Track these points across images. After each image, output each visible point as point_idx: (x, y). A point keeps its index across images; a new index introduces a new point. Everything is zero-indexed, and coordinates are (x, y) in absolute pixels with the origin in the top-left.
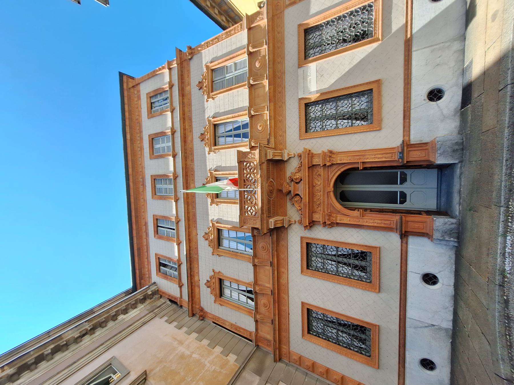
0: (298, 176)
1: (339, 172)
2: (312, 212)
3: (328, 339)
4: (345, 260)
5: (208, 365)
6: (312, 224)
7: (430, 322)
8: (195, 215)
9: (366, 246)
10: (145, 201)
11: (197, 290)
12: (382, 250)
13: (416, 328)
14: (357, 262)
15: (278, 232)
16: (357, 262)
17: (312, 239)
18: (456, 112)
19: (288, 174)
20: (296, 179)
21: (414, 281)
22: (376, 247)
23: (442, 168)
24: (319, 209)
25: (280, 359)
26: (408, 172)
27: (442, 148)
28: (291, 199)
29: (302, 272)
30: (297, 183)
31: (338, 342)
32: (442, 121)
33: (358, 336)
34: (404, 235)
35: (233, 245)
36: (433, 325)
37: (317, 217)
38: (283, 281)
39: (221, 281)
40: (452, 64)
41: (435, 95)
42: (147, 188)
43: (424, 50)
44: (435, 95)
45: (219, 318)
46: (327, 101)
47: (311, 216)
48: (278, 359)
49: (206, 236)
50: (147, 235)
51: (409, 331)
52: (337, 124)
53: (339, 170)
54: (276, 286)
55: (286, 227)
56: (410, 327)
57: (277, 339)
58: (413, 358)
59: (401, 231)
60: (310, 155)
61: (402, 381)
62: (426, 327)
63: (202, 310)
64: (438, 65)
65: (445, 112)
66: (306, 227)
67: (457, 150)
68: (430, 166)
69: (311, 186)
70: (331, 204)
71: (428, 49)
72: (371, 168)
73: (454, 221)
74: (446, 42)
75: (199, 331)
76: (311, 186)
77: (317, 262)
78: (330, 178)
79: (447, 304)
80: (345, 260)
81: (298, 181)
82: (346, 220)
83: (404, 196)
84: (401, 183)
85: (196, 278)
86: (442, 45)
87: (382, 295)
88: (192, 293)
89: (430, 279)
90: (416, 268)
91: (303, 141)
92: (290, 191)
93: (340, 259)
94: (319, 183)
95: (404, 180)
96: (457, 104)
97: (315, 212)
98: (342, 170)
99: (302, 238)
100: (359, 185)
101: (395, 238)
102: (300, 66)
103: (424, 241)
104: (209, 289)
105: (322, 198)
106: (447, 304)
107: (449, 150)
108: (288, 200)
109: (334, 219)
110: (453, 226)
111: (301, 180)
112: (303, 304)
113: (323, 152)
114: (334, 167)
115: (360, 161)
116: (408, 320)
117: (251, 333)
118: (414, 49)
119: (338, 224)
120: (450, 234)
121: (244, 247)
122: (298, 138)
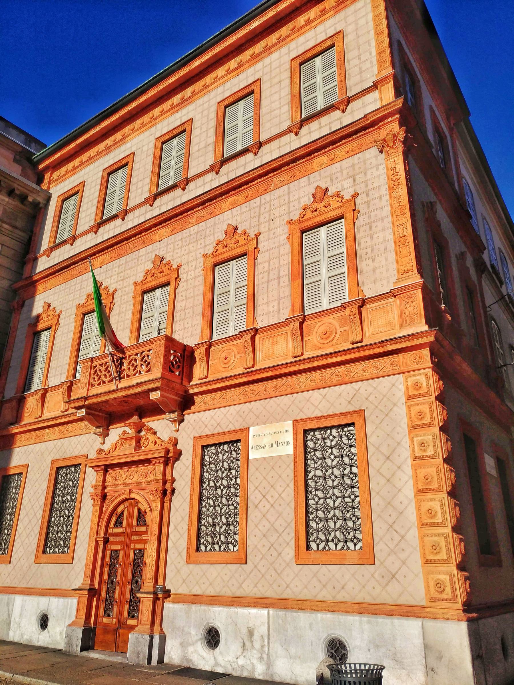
7: (12, 619)
27: (143, 640)
40: (241, 662)
43: (266, 625)
44: (212, 638)
56: (8, 599)
65: (191, 649)
67: (139, 657)
71: (266, 632)
74: (268, 655)
78: (142, 492)
79: (25, 637)
86: (266, 649)
96: (195, 663)
106: (25, 637)
107: (140, 649)
118: (272, 611)
120: (69, 644)
122: (197, 435)
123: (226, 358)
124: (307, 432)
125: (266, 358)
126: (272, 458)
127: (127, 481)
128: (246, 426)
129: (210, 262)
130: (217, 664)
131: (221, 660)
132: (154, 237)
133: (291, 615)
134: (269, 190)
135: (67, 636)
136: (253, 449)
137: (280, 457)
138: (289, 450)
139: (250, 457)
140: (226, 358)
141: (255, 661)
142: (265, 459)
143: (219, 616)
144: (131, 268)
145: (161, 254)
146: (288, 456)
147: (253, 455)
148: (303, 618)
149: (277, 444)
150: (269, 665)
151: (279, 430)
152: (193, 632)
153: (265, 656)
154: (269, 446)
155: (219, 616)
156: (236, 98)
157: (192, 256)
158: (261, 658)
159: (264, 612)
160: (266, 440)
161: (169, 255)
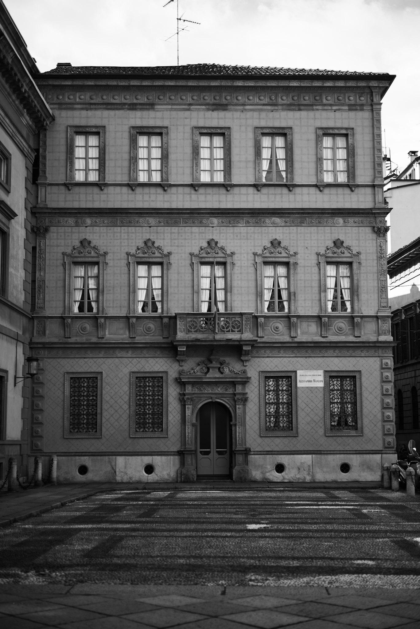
0: (226, 370)
1: (229, 407)
2: (193, 384)
6: (180, 383)
7: (117, 470)
8: (176, 224)
9: (167, 428)
12: (167, 439)
13: (110, 462)
15: (171, 349)
18: (266, 479)
19: (227, 360)
20: (223, 368)
21: (147, 460)
22: (167, 434)
23: (229, 476)
24: (196, 390)
25: (31, 348)
26: (227, 456)
28: (203, 362)
30: (219, 368)
32: (262, 473)
34: (181, 453)
35: (142, 283)
36: (115, 472)
37: (189, 389)
38: (119, 353)
40: (298, 476)
41: (280, 468)
42: (209, 114)
46: (290, 395)
47: (189, 383)
48: (32, 346)
50: (133, 107)
51: (106, 458)
52: (269, 403)
53: (231, 406)
54: (113, 346)
55: (177, 358)
57: (55, 346)
58: (86, 461)
59: (184, 451)
60: (245, 382)
61: (62, 454)
62: (113, 468)
63: (46, 230)
64: (299, 469)
65: (268, 474)
68: (231, 468)
69: (216, 383)
70: (201, 400)
72: (231, 430)
73: (195, 479)
74: (312, 472)
76: (216, 383)
81: (221, 370)
82: (188, 412)
83: (208, 453)
84: (217, 451)
88: (66, 213)
89: (149, 469)
90: (157, 461)
91: (257, 374)
92: (211, 362)
95: (219, 453)
97: (193, 387)
98: (230, 409)
99: (166, 372)
100: (217, 423)
102: (325, 372)
103: (177, 466)
104: (77, 244)
105: (206, 392)
108: (202, 359)
109: (189, 403)
110: (191, 479)
111: (222, 373)
113: (247, 393)
114: (233, 403)
115: (237, 422)
116: (114, 457)
118: (314, 456)
121: (143, 299)
122: (261, 370)
123: (277, 328)
125: (303, 333)
126: (312, 387)
127: (210, 391)
128: (295, 370)
129: (259, 260)
130: (284, 478)
131: (286, 477)
133: (323, 457)
134: (303, 225)
136: (300, 382)
137: (316, 387)
138: (322, 385)
139: (298, 386)
140: (277, 328)
141: (305, 476)
142: (307, 387)
143: (284, 459)
144: (185, 239)
145: (216, 238)
146: (321, 387)
147: (299, 385)
148: (330, 457)
149: (314, 381)
150: (313, 476)
151: (316, 374)
152: (269, 467)
153: (311, 473)
154: (310, 381)
155: (284, 459)
156: (271, 132)
157: (244, 250)
158: (309, 474)
159: (310, 456)
161: (222, 241)
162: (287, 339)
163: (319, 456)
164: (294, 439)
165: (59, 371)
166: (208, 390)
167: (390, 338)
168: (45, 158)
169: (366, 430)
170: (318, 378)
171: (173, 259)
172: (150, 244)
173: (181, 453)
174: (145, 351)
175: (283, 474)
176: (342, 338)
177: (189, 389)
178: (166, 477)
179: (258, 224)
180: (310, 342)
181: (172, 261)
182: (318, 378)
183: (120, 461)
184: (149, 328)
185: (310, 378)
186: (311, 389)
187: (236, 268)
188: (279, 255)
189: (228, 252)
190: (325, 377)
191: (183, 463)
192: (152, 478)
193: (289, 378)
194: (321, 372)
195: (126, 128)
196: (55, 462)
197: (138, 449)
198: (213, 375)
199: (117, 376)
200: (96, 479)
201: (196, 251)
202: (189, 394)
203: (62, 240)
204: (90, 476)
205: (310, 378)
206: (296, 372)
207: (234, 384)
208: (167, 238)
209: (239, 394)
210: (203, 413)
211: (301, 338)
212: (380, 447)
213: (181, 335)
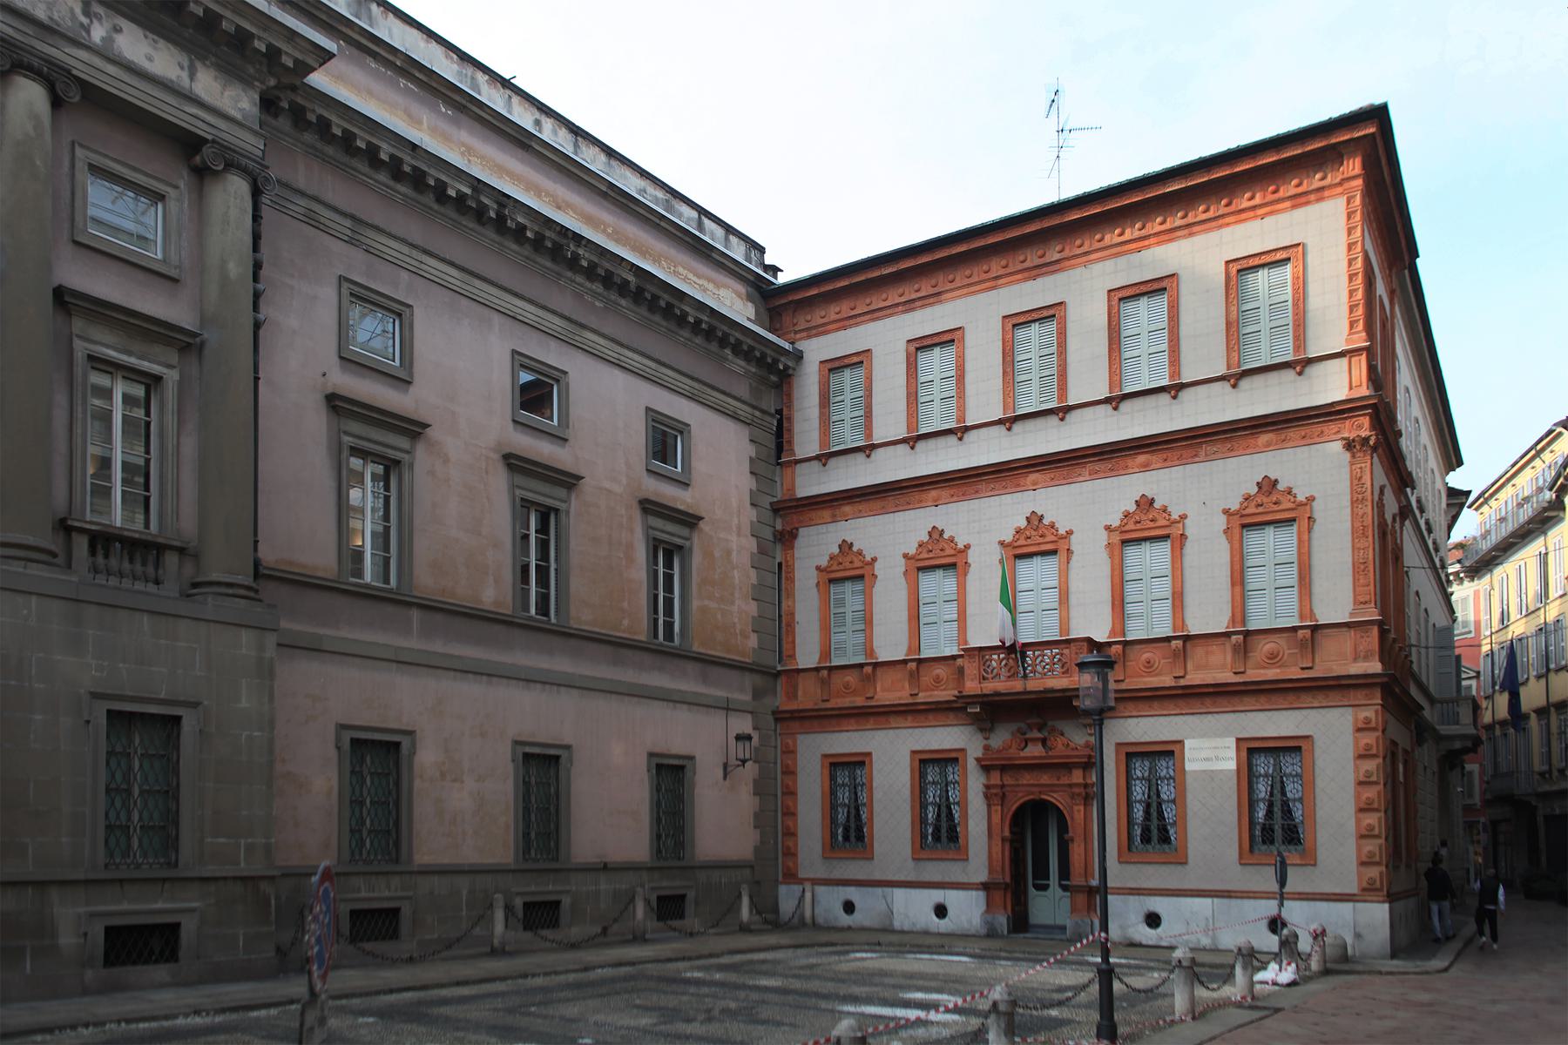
2: (1004, 769)
3: (833, 793)
4: (943, 815)
5: (735, 608)
6: (986, 768)
8: (976, 495)
10: (994, 283)
11: (826, 514)
14: (944, 831)
16: (944, 831)
17: (965, 768)
21: (937, 896)
29: (914, 752)
30: (1044, 741)
31: (833, 807)
33: (850, 832)
34: (985, 887)
38: (894, 721)
39: (861, 577)
41: (1153, 920)
45: (793, 581)
49: (936, 536)
51: (879, 891)
58: (852, 893)
66: (978, 760)
75: (762, 551)
77: (932, 774)
80: (943, 815)
83: (1045, 888)
85: (847, 509)
87: (910, 863)
89: (941, 911)
90: (952, 898)
93: (944, 809)
94: (1045, 779)
99: (963, 750)
101: (983, 876)
102: (1238, 740)
103: (984, 908)
112: (869, 754)
117: (793, 656)
119: (989, 806)
124: (1252, 750)
129: (1117, 538)
132: (1022, 481)
133: (1234, 902)
135: (987, 923)
138: (1232, 765)
147: (1189, 766)
148: (1248, 904)
149: (1217, 758)
150: (1214, 938)
159: (1209, 900)
160: (1204, 754)
162: (1167, 681)
163: (1225, 901)
164: (1180, 867)
165: (814, 748)
166: (1027, 779)
167: (1375, 667)
168: (790, 419)
169: (1322, 854)
170: (1222, 753)
171: (972, 557)
172: (936, 536)
173: (985, 887)
174: (931, 716)
175: (1159, 930)
176: (1272, 674)
177: (996, 778)
178: (966, 925)
179: (1113, 472)
180: (1207, 686)
181: (970, 560)
182: (1222, 753)
183: (899, 894)
184: (938, 676)
185: (1210, 751)
186: (1211, 775)
187: (1074, 558)
188: (1276, 508)
189: (1062, 531)
190: (1238, 749)
191: (989, 904)
192: (943, 925)
193: (1169, 752)
194: (1232, 742)
195: (902, 346)
196: (808, 895)
197: (927, 877)
198: (1035, 751)
199: (892, 754)
200: (867, 923)
201: (1008, 537)
202: (995, 786)
203: (817, 544)
204: (857, 919)
205: (1210, 751)
206: (1181, 742)
207: (1068, 767)
208: (1060, 503)
209: (1077, 785)
210: (1018, 820)
211: (1195, 678)
212: (1353, 888)
213: (971, 686)
